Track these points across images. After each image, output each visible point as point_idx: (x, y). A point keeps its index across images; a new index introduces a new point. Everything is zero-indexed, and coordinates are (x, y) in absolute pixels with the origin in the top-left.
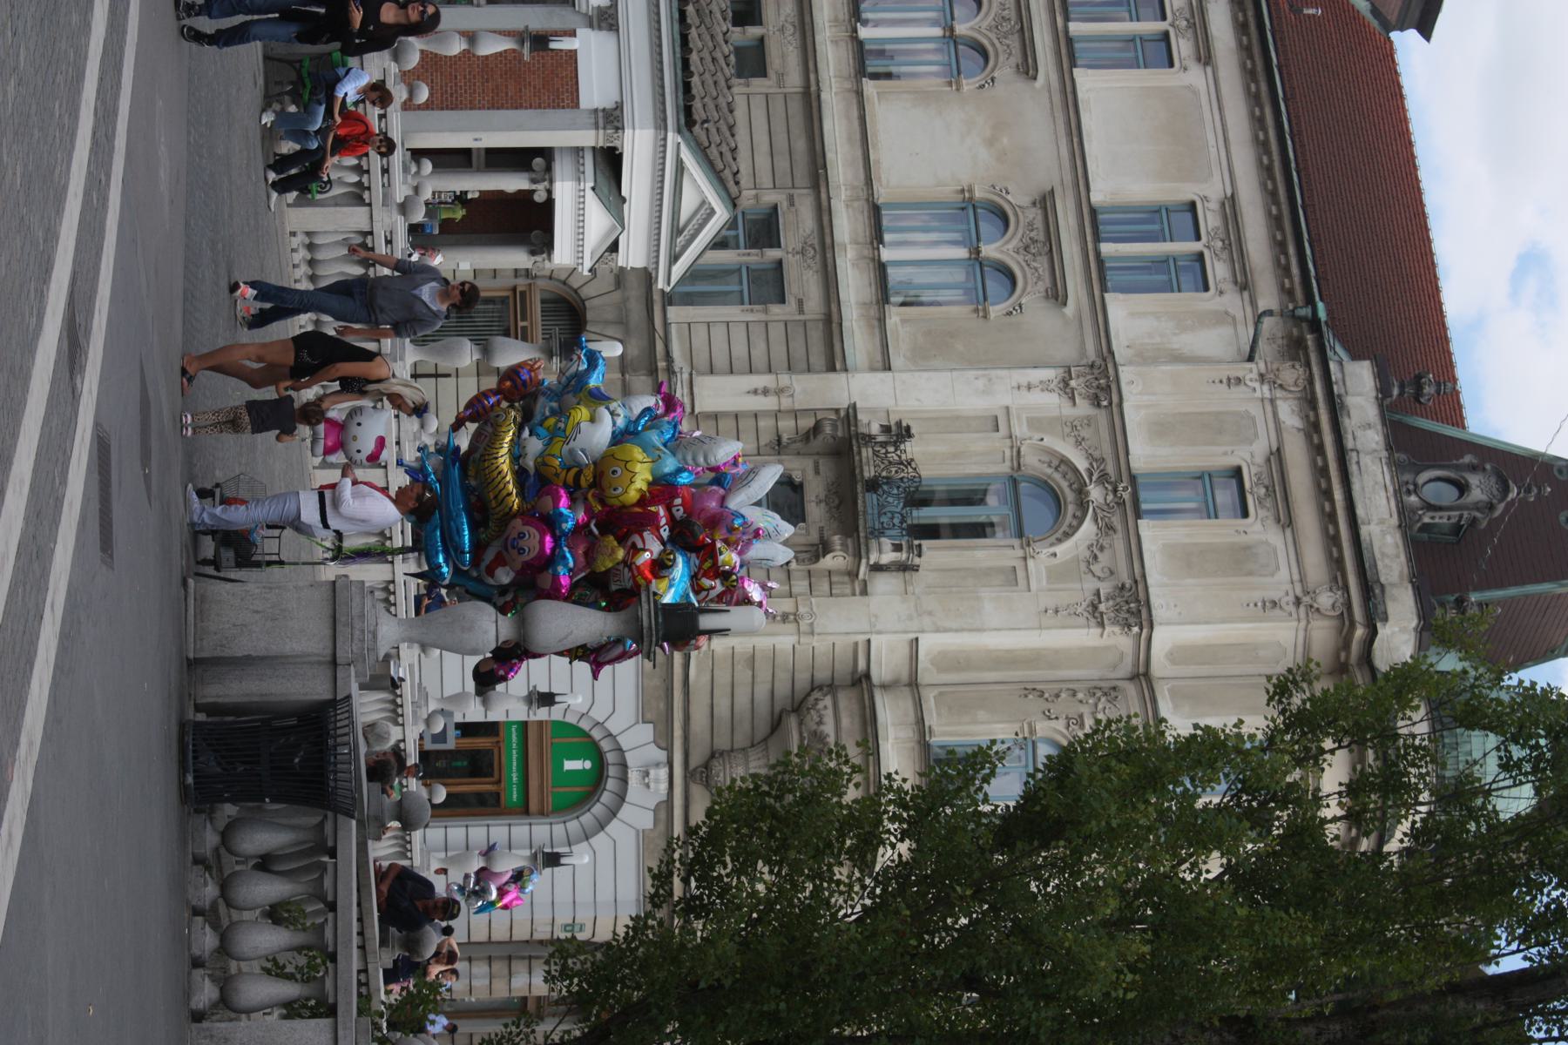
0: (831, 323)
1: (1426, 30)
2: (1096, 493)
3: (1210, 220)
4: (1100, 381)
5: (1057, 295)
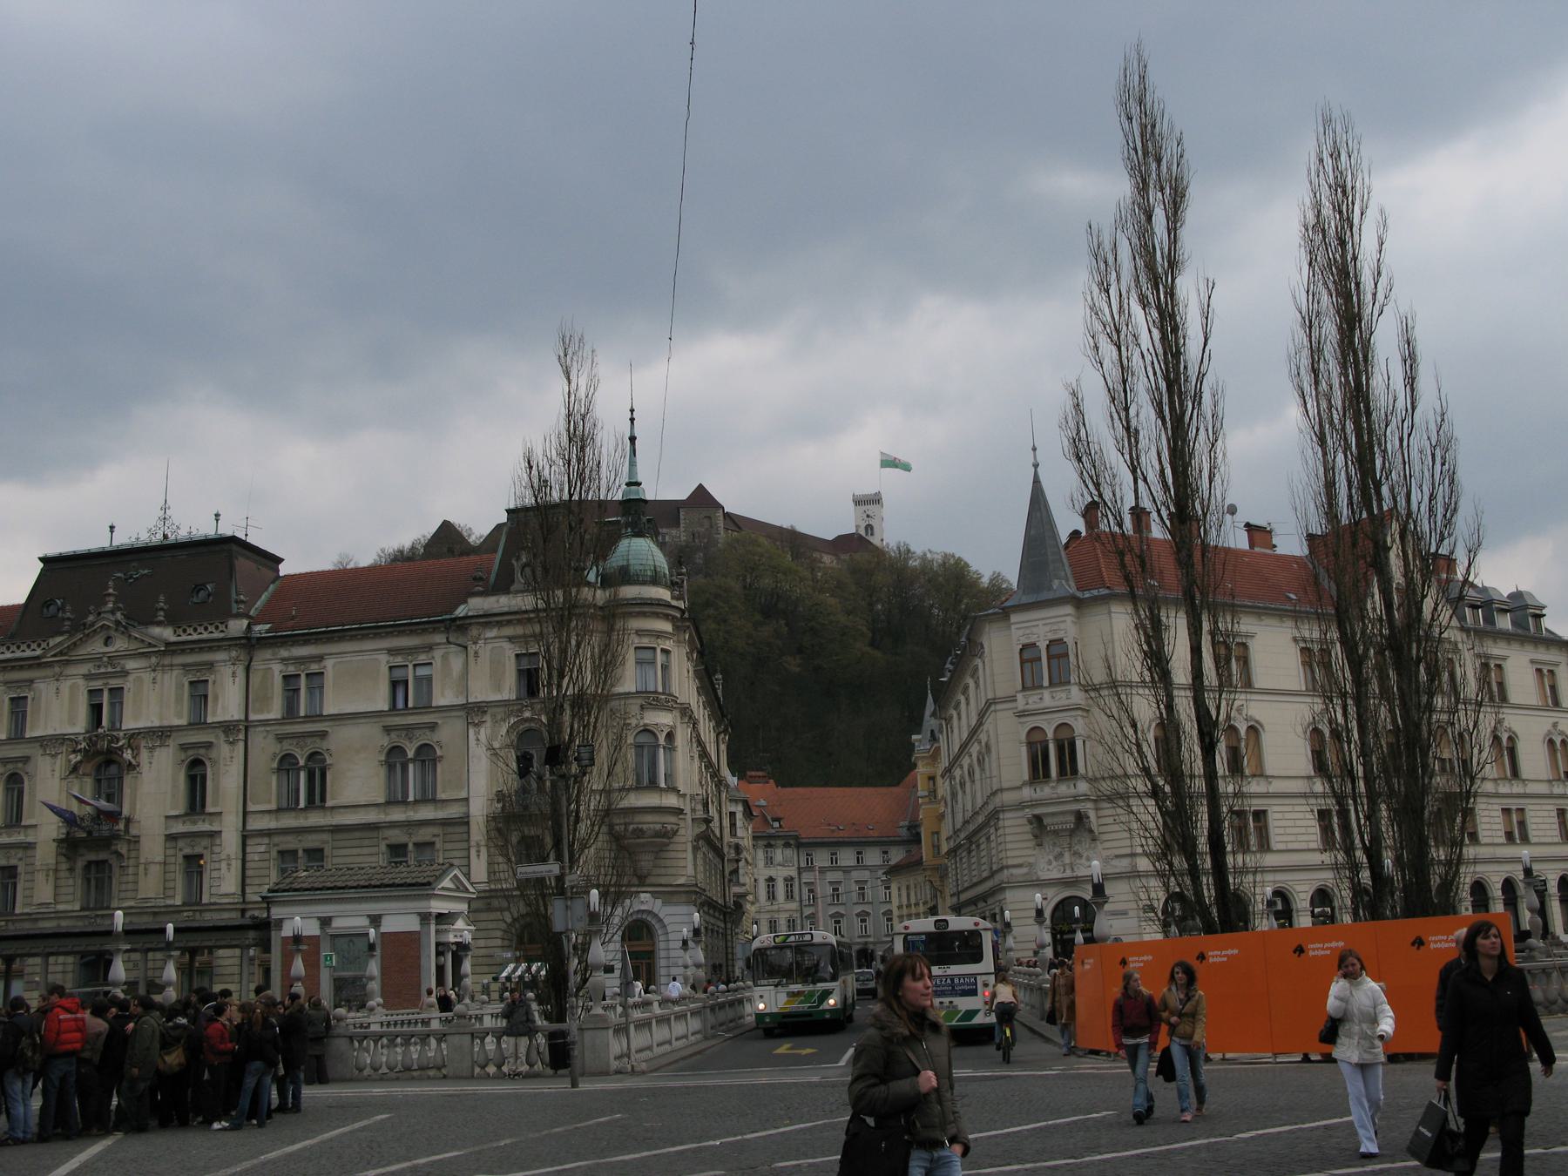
0: (445, 823)
1: (280, 560)
2: (527, 714)
3: (399, 660)
4: (473, 712)
5: (433, 727)
